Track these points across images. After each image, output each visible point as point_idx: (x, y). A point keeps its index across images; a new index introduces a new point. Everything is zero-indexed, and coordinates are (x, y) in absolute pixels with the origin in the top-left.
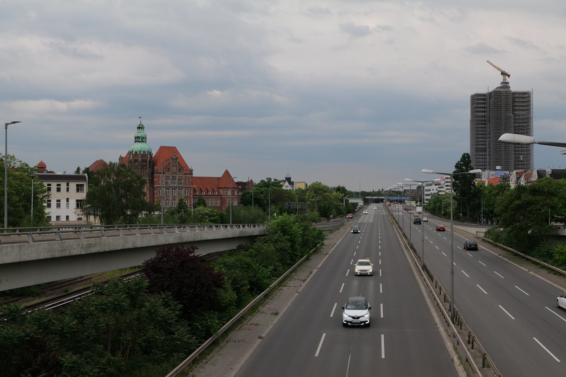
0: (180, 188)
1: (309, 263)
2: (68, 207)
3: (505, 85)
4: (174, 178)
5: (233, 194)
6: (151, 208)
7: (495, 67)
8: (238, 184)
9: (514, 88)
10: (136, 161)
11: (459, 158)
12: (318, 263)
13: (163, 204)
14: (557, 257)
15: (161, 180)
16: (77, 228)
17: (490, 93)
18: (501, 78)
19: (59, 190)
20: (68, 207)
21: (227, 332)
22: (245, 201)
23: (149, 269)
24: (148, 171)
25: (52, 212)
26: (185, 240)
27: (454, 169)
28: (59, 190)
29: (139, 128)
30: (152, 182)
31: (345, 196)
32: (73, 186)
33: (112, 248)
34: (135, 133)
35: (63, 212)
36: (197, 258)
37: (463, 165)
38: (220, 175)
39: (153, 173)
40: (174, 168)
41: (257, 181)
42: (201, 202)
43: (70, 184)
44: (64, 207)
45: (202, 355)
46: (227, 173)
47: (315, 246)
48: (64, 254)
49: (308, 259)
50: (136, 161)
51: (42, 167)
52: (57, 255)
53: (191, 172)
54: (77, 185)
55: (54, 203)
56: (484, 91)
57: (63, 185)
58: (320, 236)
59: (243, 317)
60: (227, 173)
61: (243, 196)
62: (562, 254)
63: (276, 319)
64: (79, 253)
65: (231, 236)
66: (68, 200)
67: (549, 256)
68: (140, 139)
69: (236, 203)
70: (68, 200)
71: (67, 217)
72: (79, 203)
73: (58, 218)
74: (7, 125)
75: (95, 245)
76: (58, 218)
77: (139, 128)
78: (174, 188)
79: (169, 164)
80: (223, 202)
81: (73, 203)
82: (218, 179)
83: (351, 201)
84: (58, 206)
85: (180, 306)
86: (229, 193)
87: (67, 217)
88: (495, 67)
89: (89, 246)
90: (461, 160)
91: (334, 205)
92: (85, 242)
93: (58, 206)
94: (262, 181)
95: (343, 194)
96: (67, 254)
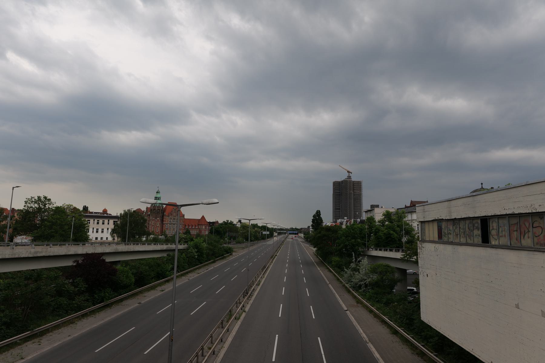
0: (174, 224)
1: (213, 264)
2: (108, 233)
3: (349, 177)
4: (174, 219)
5: (206, 228)
6: (148, 234)
8: (210, 223)
9: (354, 179)
10: (154, 209)
12: (219, 264)
13: (167, 232)
14: (333, 263)
15: (167, 220)
16: (109, 243)
18: (347, 173)
19: (103, 223)
20: (108, 233)
21: (121, 300)
22: (211, 232)
23: (78, 265)
24: (161, 215)
25: (92, 235)
26: (120, 251)
28: (103, 223)
29: (157, 193)
30: (162, 221)
32: (111, 221)
33: (55, 254)
34: (155, 195)
35: (99, 235)
36: (104, 260)
38: (200, 218)
39: (163, 216)
40: (175, 214)
41: (220, 221)
42: (187, 232)
43: (110, 221)
44: (100, 234)
45: (93, 312)
46: (203, 217)
47: (223, 255)
48: (13, 257)
49: (214, 262)
50: (154, 209)
51: (105, 211)
52: (7, 257)
53: (184, 215)
54: (114, 221)
55: (100, 230)
56: (339, 180)
57: (106, 221)
58: (229, 251)
59: (141, 292)
60: (203, 217)
61: (212, 229)
62: (335, 262)
63: (160, 293)
64: (27, 256)
65: (160, 249)
66: (108, 229)
67: (330, 263)
68: (156, 198)
69: (207, 233)
70: (108, 229)
71: (107, 238)
72: (114, 231)
73: (102, 238)
74: (13, 188)
75: (41, 252)
76: (102, 238)
77: (157, 193)
78: (174, 224)
79: (172, 211)
80: (200, 231)
81: (110, 230)
82: (199, 220)
83: (264, 233)
84: (102, 232)
85: (87, 286)
86: (204, 227)
87: (107, 238)
89: (36, 252)
91: (254, 234)
92: (33, 250)
93: (102, 232)
94: (224, 222)
96: (17, 256)
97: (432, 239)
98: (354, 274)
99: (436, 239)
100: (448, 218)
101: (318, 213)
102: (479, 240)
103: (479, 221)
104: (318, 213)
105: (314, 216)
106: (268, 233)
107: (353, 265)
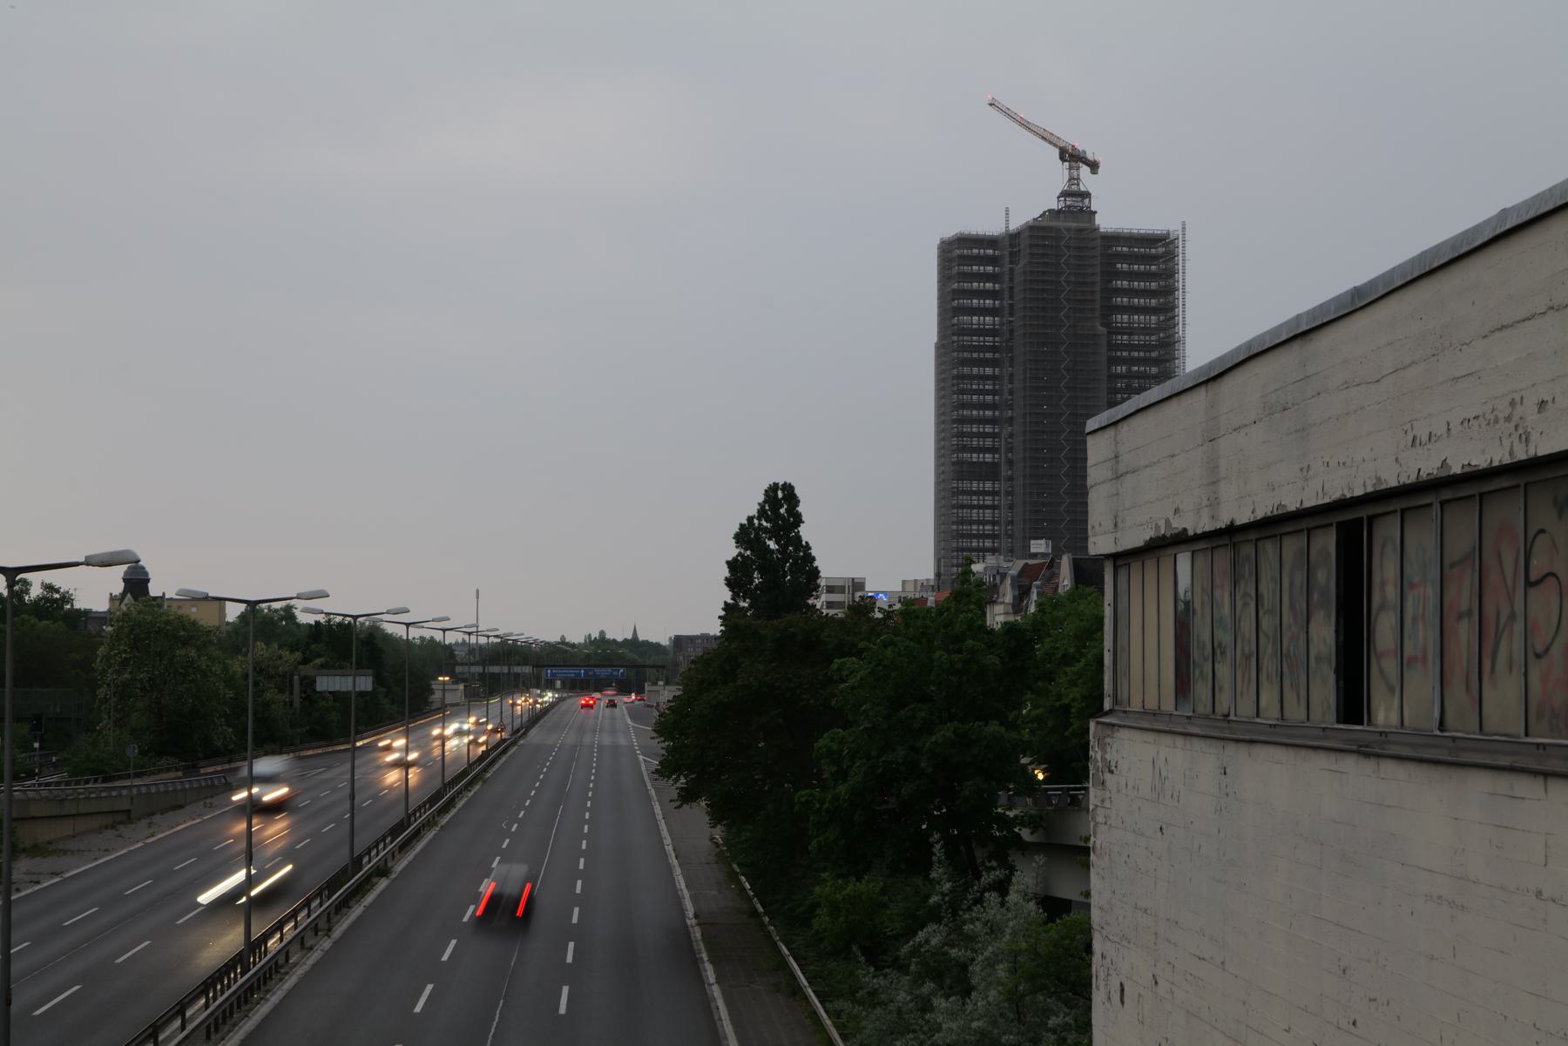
3: (1076, 204)
7: (1026, 125)
9: (1110, 218)
11: (749, 505)
14: (822, 920)
17: (1013, 238)
18: (1057, 176)
27: (732, 551)
31: (305, 661)
37: (773, 534)
56: (992, 226)
88: (1026, 125)
90: (762, 513)
95: (298, 655)
97: (1151, 704)
98: (926, 1006)
99: (1168, 705)
100: (1205, 525)
101: (781, 506)
102: (1325, 692)
103: (1327, 542)
104: (781, 506)
105: (744, 536)
106: (365, 683)
107: (933, 935)
